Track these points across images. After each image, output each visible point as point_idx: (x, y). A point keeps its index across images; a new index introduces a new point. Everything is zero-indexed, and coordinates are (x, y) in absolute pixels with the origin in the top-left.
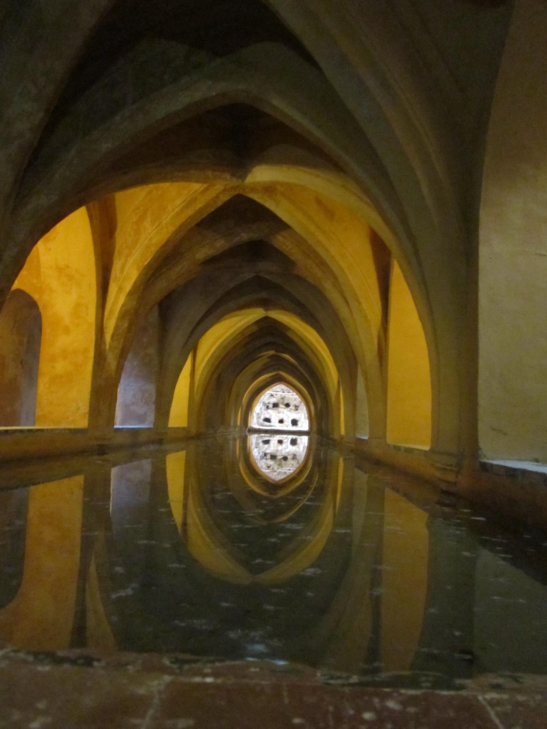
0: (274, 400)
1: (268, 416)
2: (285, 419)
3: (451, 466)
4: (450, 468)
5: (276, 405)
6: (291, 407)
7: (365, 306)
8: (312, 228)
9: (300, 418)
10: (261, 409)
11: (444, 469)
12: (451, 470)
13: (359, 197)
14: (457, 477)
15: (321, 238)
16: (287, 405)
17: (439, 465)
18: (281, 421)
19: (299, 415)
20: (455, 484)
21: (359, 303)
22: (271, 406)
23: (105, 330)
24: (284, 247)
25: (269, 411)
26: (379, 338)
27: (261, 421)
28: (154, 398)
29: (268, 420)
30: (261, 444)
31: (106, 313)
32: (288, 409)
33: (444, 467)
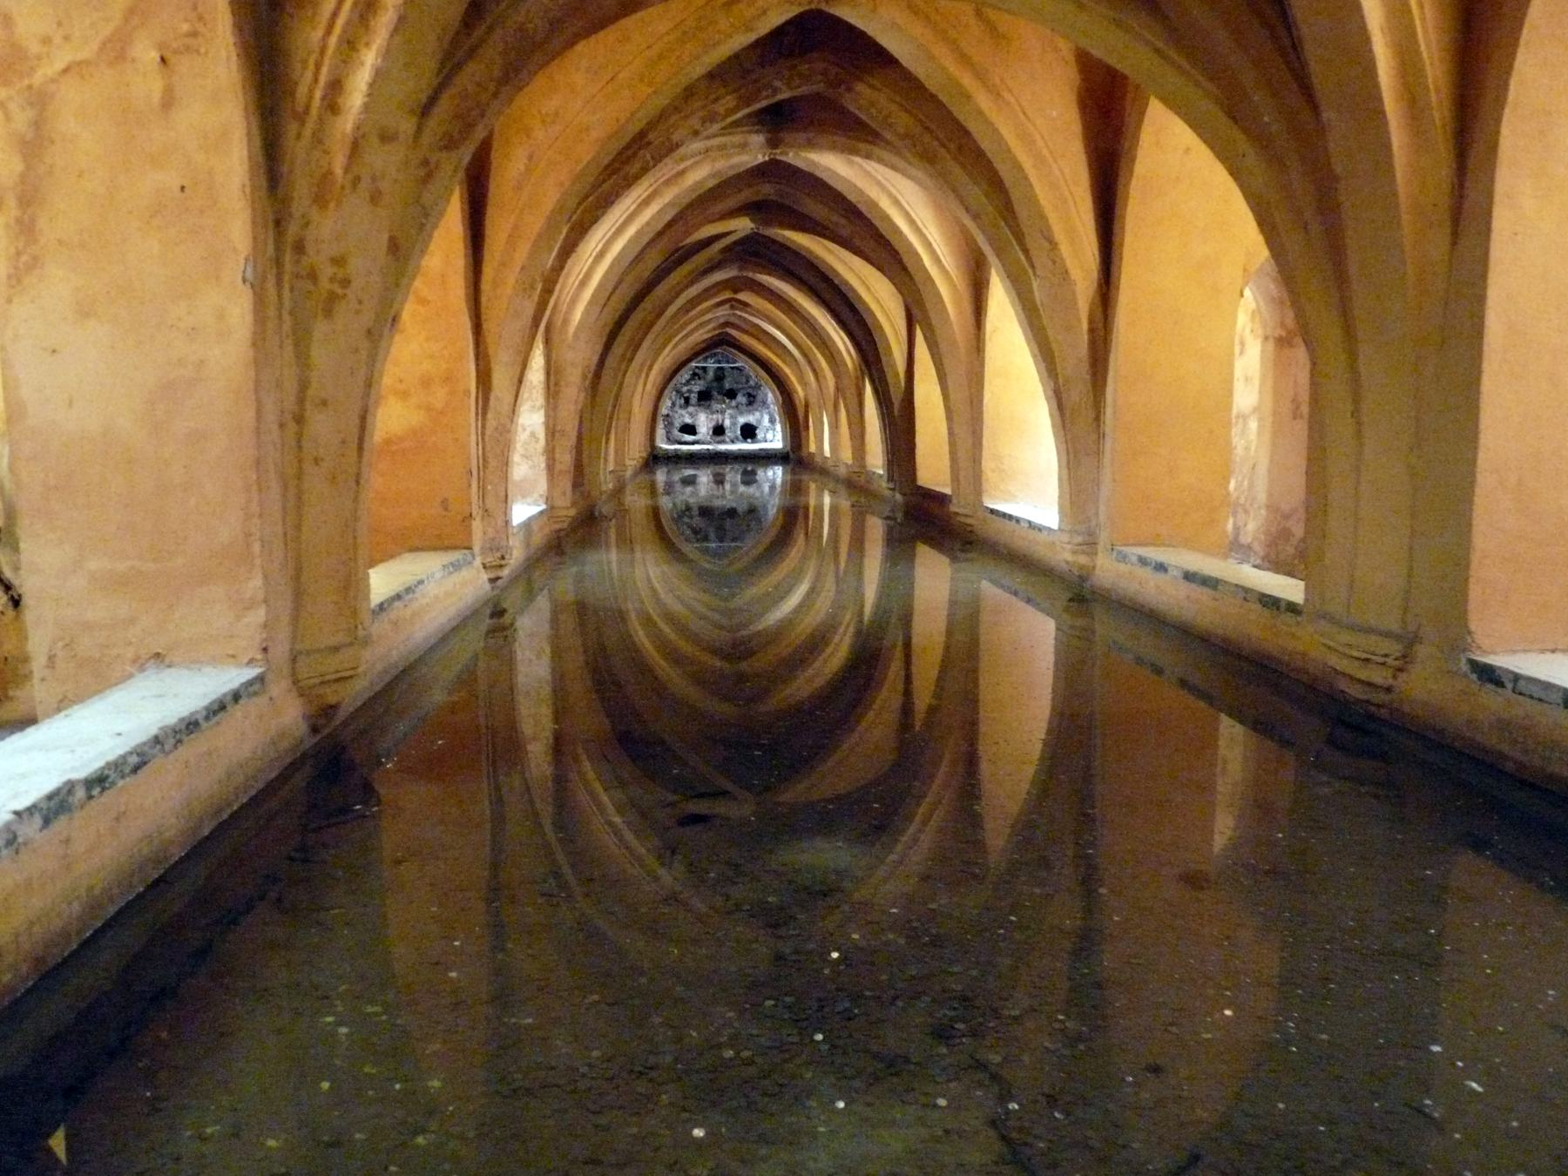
0: (697, 387)
1: (688, 420)
2: (727, 423)
3: (1386, 656)
4: (1381, 660)
5: (705, 397)
6: (741, 399)
7: (1065, 249)
8: (967, 81)
9: (759, 421)
10: (674, 404)
11: (1367, 660)
12: (1383, 664)
13: (1157, 51)
14: (1395, 677)
15: (983, 101)
16: (731, 394)
17: (1355, 654)
18: (719, 431)
19: (757, 414)
20: (1389, 690)
21: (1053, 245)
22: (694, 398)
23: (484, 326)
24: (873, 110)
25: (691, 409)
26: (1091, 321)
27: (676, 433)
28: (542, 442)
29: (690, 429)
30: (678, 487)
31: (486, 286)
32: (734, 403)
33: (1364, 656)
